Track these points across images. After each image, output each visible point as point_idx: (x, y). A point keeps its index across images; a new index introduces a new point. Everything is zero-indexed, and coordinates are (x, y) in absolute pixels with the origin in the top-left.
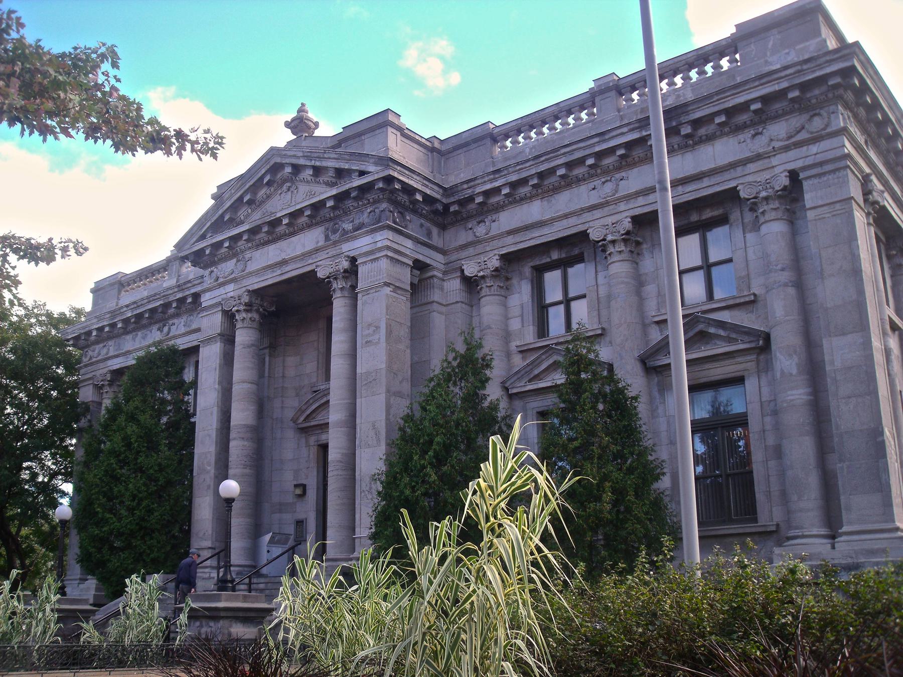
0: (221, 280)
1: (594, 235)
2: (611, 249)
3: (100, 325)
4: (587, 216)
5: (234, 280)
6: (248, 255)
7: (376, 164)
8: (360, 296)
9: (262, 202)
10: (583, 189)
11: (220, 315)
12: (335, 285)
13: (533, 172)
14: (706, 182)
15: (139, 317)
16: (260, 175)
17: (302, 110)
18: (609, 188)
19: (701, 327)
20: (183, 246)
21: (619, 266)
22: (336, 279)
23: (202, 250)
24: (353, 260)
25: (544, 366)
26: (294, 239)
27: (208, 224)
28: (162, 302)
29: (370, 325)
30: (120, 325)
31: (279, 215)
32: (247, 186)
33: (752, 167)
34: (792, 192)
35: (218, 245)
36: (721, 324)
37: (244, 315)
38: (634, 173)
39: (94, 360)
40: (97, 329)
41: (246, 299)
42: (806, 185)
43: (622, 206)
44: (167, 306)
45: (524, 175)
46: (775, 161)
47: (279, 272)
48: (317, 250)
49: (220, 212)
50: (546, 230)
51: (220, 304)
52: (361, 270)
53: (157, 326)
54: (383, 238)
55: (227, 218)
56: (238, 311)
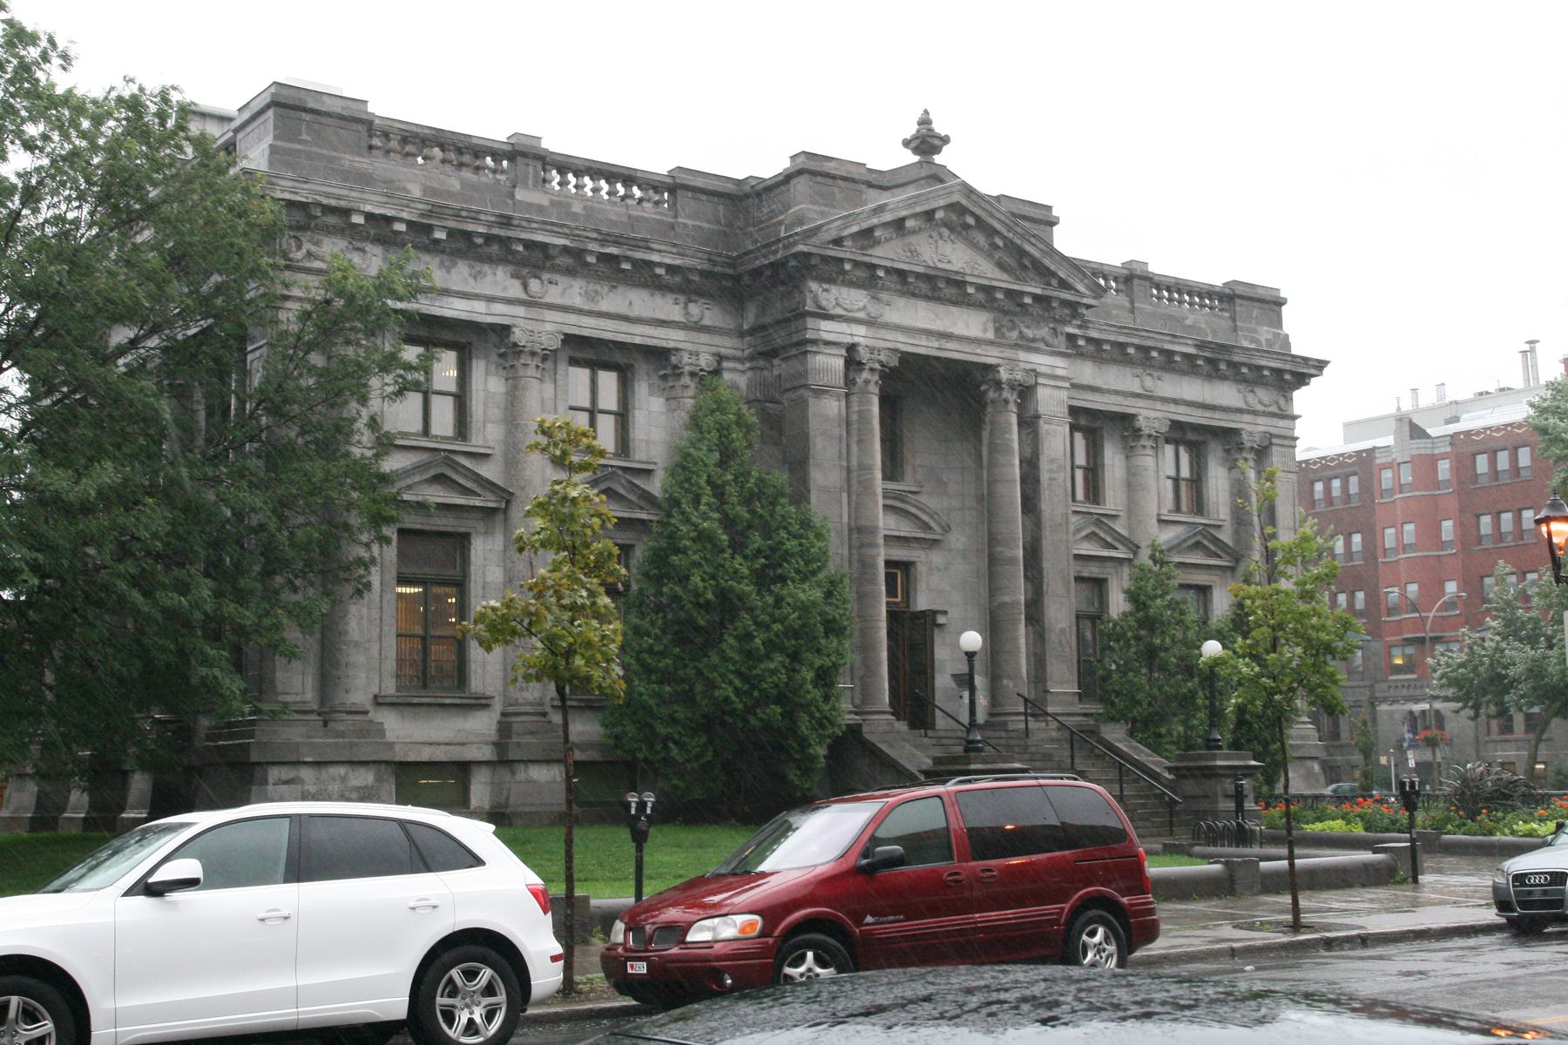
0: (839, 311)
1: (1141, 422)
2: (1143, 442)
3: (389, 213)
4: (1131, 401)
5: (870, 323)
6: (884, 296)
7: (1088, 287)
8: (1041, 422)
9: (914, 232)
10: (1128, 371)
11: (841, 362)
12: (1006, 394)
13: (1112, 338)
14: (1217, 415)
15: (489, 239)
16: (936, 205)
17: (925, 121)
18: (1149, 382)
19: (1199, 538)
20: (809, 237)
21: (1147, 460)
22: (1013, 388)
23: (841, 260)
24: (1037, 374)
25: (1084, 533)
26: (954, 310)
27: (855, 229)
28: (567, 242)
29: (1052, 461)
30: (440, 235)
31: (968, 279)
32: (918, 209)
33: (1247, 418)
34: (1262, 453)
35: (856, 264)
36: (1216, 541)
37: (876, 377)
38: (1167, 377)
39: (317, 264)
40: (369, 217)
41: (895, 362)
42: (1274, 449)
43: (1159, 405)
44: (566, 250)
45: (1104, 336)
46: (1260, 420)
47: (936, 344)
48: (992, 343)
49: (875, 221)
50: (1097, 397)
51: (851, 348)
52: (1043, 394)
53: (511, 268)
54: (1060, 365)
55: (877, 233)
56: (872, 370)
